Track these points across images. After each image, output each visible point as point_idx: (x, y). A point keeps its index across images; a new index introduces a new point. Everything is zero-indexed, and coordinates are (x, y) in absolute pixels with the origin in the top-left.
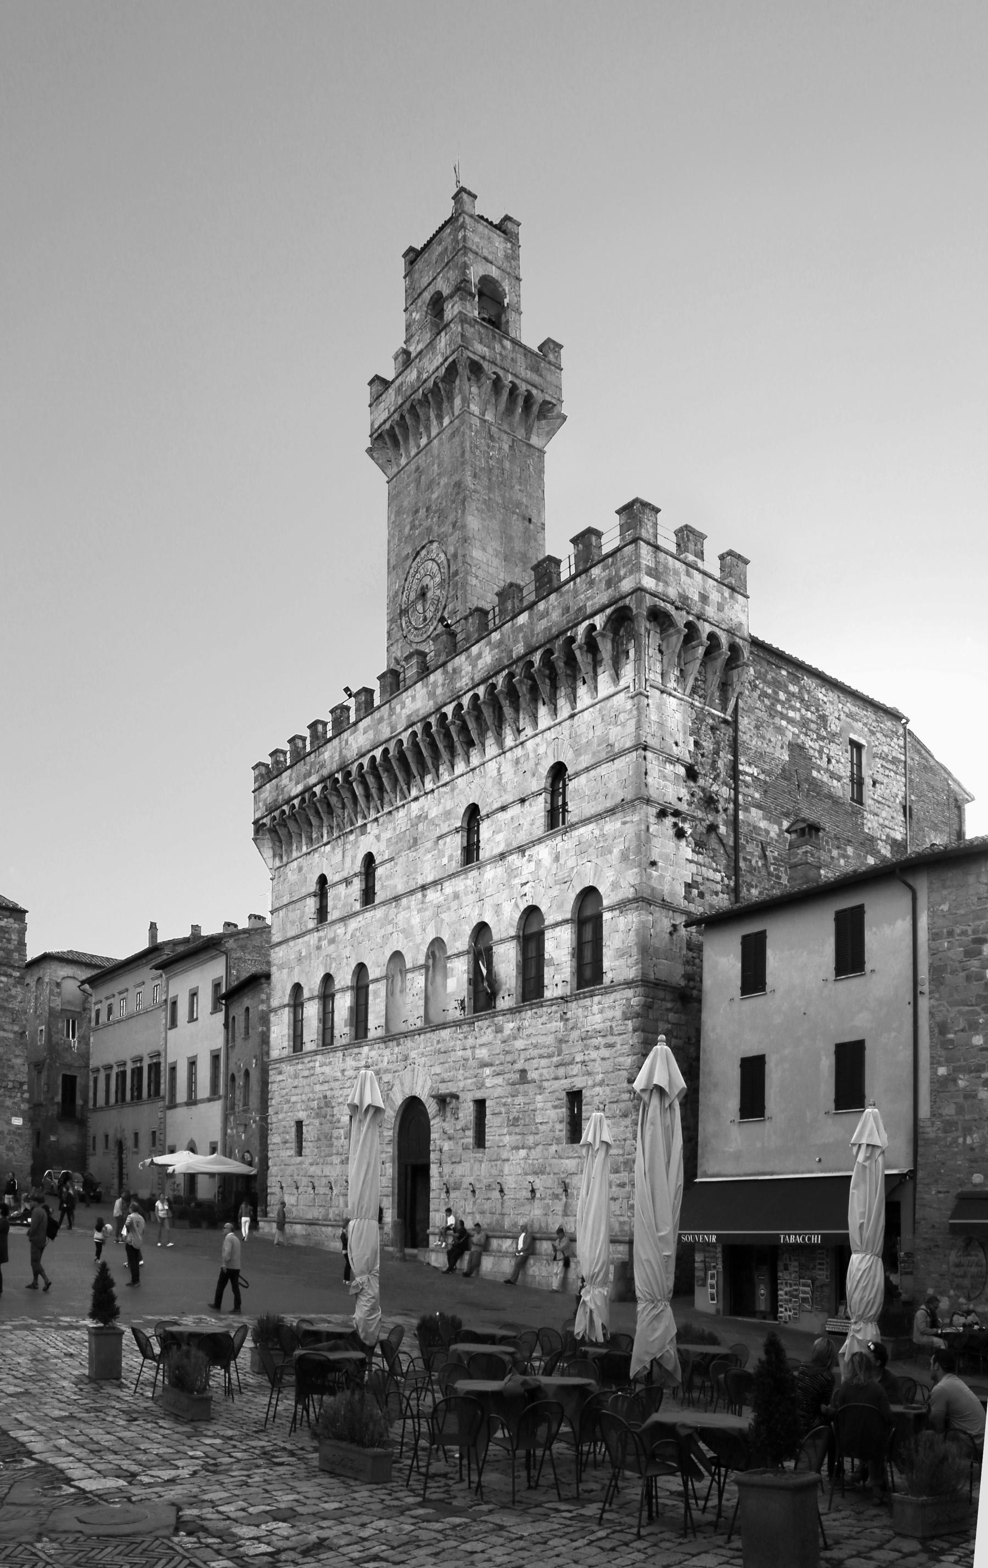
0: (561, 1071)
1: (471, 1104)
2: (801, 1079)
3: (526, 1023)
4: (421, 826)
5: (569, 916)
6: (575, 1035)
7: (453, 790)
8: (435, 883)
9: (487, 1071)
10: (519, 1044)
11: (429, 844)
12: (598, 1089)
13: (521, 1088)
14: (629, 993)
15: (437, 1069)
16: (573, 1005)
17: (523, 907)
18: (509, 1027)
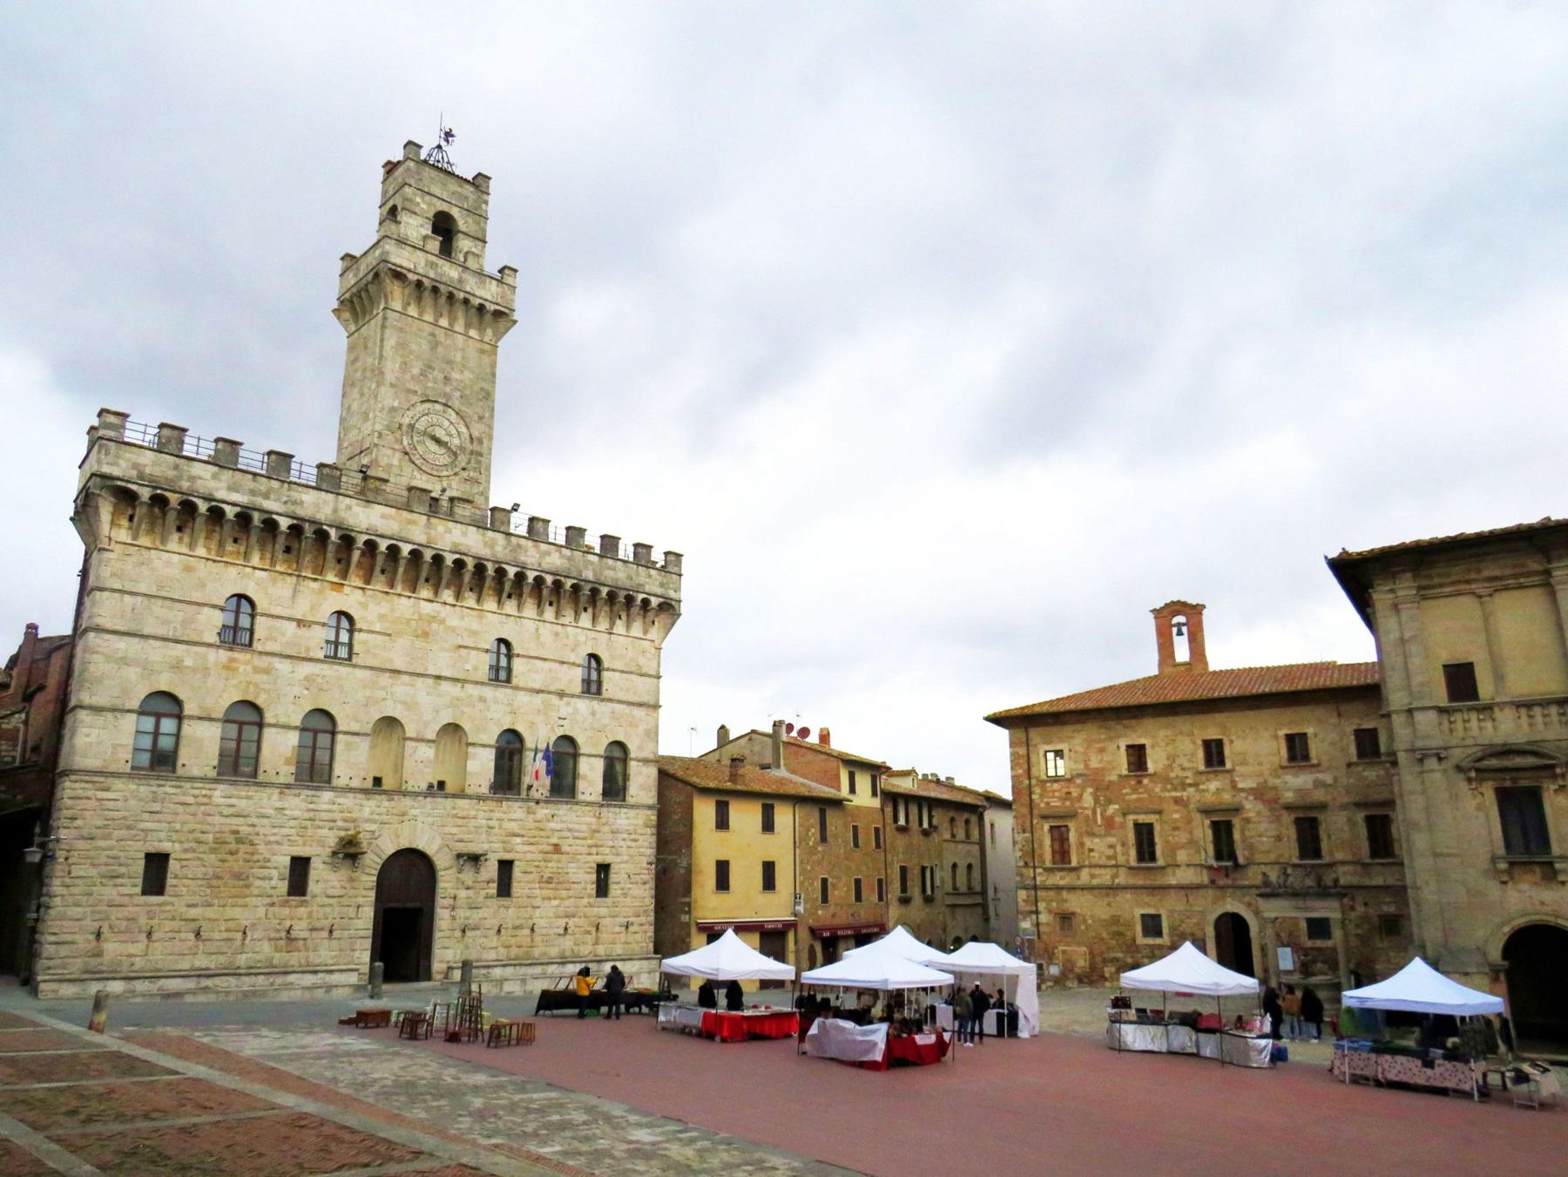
0: (594, 850)
2: (745, 876)
4: (435, 626)
6: (606, 828)
7: (481, 618)
8: (457, 680)
9: (518, 840)
10: (553, 825)
15: (454, 830)
16: (605, 810)
17: (560, 732)
18: (543, 811)
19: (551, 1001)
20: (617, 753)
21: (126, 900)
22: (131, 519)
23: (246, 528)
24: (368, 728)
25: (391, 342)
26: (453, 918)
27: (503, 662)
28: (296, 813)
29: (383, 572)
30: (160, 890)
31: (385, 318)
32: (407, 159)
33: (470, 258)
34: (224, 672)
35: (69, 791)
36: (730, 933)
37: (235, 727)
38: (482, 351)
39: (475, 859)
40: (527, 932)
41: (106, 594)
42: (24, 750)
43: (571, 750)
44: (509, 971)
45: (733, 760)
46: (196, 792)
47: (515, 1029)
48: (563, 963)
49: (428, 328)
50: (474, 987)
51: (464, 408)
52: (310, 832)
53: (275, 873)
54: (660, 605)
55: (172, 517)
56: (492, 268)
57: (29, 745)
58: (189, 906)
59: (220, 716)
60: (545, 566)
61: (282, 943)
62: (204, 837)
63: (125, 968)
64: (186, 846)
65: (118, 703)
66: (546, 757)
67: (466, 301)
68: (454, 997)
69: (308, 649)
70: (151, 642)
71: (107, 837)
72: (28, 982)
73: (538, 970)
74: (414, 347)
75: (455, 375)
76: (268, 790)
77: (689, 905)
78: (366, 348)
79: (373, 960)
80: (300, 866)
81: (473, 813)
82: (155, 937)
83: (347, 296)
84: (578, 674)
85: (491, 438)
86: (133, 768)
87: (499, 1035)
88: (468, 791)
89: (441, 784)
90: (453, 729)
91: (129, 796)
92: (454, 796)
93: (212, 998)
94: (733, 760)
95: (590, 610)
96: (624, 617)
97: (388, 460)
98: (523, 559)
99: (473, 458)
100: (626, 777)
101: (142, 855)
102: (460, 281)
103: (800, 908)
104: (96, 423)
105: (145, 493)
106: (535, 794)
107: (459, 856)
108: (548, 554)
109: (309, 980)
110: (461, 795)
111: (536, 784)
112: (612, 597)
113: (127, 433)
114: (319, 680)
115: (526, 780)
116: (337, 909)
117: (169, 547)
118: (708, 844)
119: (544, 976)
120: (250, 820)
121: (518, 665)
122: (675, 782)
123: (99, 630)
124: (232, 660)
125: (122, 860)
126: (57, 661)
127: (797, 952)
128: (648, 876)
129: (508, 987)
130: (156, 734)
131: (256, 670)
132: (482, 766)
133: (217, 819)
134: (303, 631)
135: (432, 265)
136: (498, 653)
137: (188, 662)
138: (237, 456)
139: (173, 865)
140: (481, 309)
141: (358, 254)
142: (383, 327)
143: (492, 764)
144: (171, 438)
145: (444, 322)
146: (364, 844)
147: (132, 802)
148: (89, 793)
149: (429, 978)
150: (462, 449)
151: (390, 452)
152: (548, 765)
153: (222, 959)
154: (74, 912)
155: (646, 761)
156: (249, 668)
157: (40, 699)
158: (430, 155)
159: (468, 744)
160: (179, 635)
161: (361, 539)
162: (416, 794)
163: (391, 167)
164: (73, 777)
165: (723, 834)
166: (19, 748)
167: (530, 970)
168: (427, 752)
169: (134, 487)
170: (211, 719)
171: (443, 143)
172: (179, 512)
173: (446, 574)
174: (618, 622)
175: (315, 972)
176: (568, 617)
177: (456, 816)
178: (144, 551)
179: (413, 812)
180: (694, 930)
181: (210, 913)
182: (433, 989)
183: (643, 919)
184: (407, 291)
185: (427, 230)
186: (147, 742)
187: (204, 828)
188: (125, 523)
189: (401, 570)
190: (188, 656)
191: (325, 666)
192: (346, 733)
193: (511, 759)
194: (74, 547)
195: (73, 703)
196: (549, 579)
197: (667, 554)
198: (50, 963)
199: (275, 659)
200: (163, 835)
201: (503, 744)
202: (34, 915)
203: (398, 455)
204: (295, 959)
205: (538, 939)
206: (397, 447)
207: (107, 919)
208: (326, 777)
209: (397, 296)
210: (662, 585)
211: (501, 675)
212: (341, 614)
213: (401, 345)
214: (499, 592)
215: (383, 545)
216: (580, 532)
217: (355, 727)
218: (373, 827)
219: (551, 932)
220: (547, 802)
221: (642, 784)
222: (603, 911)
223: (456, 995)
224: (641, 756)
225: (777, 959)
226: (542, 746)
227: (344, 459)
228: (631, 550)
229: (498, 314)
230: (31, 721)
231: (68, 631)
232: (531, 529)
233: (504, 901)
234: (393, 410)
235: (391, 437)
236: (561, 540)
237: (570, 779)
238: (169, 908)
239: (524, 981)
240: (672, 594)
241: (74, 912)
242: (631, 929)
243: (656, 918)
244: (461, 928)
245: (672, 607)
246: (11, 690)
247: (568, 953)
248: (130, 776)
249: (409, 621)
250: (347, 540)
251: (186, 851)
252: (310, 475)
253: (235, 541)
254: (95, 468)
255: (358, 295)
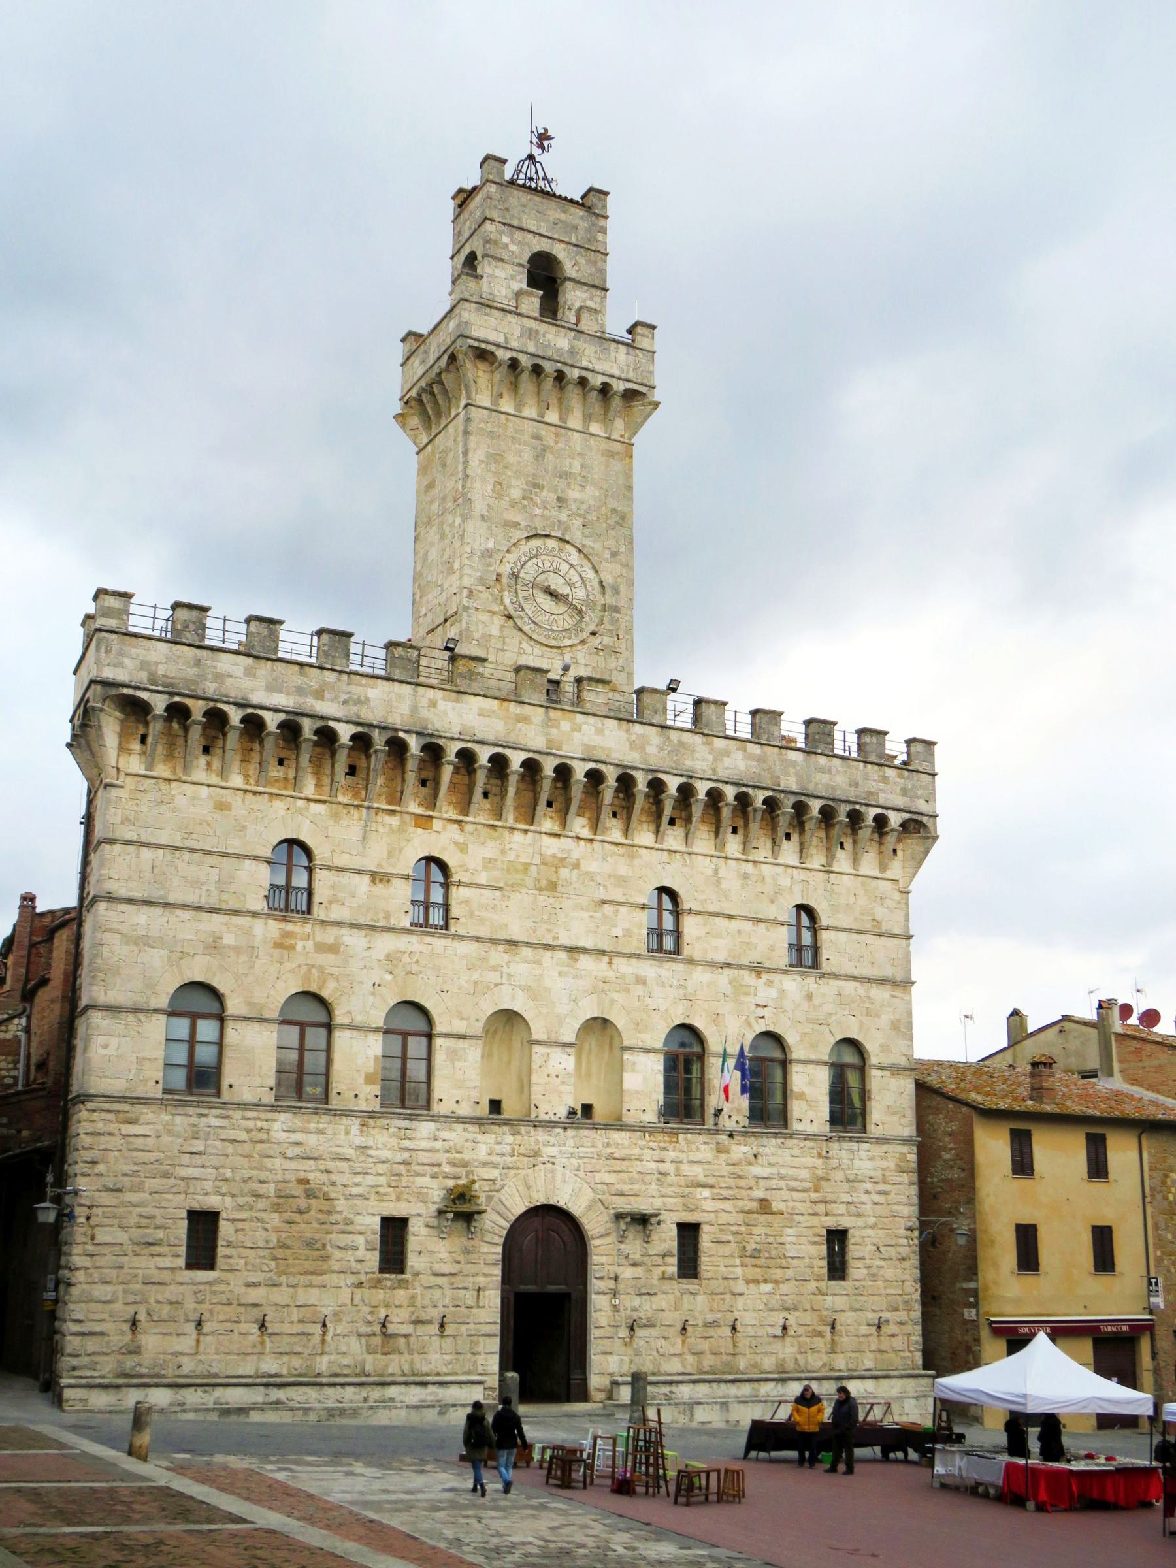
0: (821, 1208)
1: (674, 1227)
3: (767, 1150)
4: (564, 873)
5: (826, 1058)
6: (839, 1175)
7: (632, 857)
8: (599, 952)
9: (706, 1193)
10: (757, 1170)
11: (584, 902)
12: (869, 1232)
13: (763, 1218)
14: (905, 1149)
16: (836, 1145)
17: (760, 1027)
18: (740, 1150)
19: (764, 1437)
20: (850, 1058)
21: (166, 1276)
22: (143, 740)
23: (295, 743)
24: (478, 1028)
25: (477, 457)
26: (616, 1308)
27: (668, 922)
28: (385, 1154)
29: (486, 795)
30: (211, 1265)
31: (468, 420)
32: (486, 181)
33: (585, 316)
34: (276, 952)
35: (86, 1124)
36: (1042, 1339)
37: (295, 1030)
38: (611, 454)
39: (642, 1221)
40: (728, 1331)
41: (117, 848)
42: (28, 1065)
43: (778, 1054)
44: (702, 1390)
45: (1035, 1065)
46: (251, 1124)
47: (713, 1476)
48: (784, 1380)
49: (530, 427)
50: (651, 1413)
51: (587, 542)
52: (404, 1179)
53: (360, 1240)
54: (904, 825)
55: (196, 733)
56: (617, 326)
57: (34, 1060)
58: (249, 1285)
59: (275, 1015)
60: (722, 774)
61: (378, 1340)
62: (262, 1189)
63: (170, 1371)
64: (241, 1200)
65: (140, 1000)
66: (740, 1066)
67: (583, 382)
68: (621, 1426)
69: (387, 916)
70: (179, 912)
71: (139, 1188)
72: (50, 1388)
73: (746, 1390)
74: (510, 458)
75: (574, 494)
76: (345, 1120)
77: (975, 1293)
78: (444, 465)
79: (503, 1368)
80: (394, 1230)
81: (636, 1151)
82: (207, 1327)
83: (414, 393)
84: (783, 937)
85: (630, 583)
86: (165, 1091)
87: (691, 1487)
88: (628, 1119)
89: (587, 1109)
90: (600, 1025)
91: (165, 1128)
92: (607, 1127)
93: (285, 1417)
94: (1035, 1065)
95: (795, 837)
96: (848, 845)
97: (482, 630)
98: (688, 763)
99: (605, 615)
100: (864, 1095)
101: (185, 1215)
102: (572, 352)
103: (1158, 1301)
104: (91, 608)
105: (159, 704)
106: (727, 1123)
107: (619, 1217)
108: (727, 753)
109: (415, 1395)
110: (616, 1124)
111: (727, 1107)
112: (827, 814)
113: (133, 620)
114: (406, 959)
115: (714, 1100)
116: (449, 1293)
117: (194, 778)
118: (1001, 1202)
119: (755, 1400)
120: (323, 1165)
121: (690, 926)
122: (941, 1099)
123: (110, 898)
124: (287, 935)
125: (159, 1221)
126: (62, 940)
127: (1156, 1371)
128: (908, 1248)
129: (701, 1414)
130: (192, 1042)
131: (321, 948)
132: (644, 1082)
133: (278, 1163)
134: (379, 889)
135: (531, 334)
136: (660, 909)
137: (229, 939)
138: (276, 640)
139: (225, 1229)
140: (605, 390)
141: (425, 332)
142: (466, 433)
143: (660, 1079)
144: (188, 622)
145: (552, 417)
146: (482, 1200)
147: (166, 1139)
148: (113, 1127)
149: (584, 1397)
150: (591, 603)
151: (485, 617)
152: (743, 1077)
153: (296, 1362)
154: (100, 1291)
155: (895, 1070)
156: (310, 945)
157: (43, 995)
158: (518, 172)
159: (624, 1049)
160: (213, 902)
161: (452, 749)
162: (553, 1124)
163: (464, 198)
164: (90, 1105)
165: (1023, 1183)
166: (21, 1065)
167: (733, 1390)
168: (563, 1062)
169: (144, 695)
170: (263, 1020)
171: (536, 151)
172: (205, 727)
173: (577, 792)
174: (840, 853)
175: (424, 1384)
176: (763, 850)
177: (611, 1157)
178: (163, 785)
179: (549, 1151)
180: (985, 1333)
181: (280, 1296)
182: (590, 1415)
183: (902, 1315)
184: (497, 376)
185: (521, 283)
186: (180, 1054)
187: (263, 1175)
188: (136, 746)
189: (511, 791)
190: (228, 930)
191: (414, 939)
192: (448, 1036)
193: (688, 1070)
194: (73, 784)
195: (84, 1001)
196: (730, 792)
197: (909, 742)
198: (75, 1362)
199: (345, 931)
200: (209, 1186)
201: (674, 1047)
202: (51, 1295)
203: (499, 620)
204: (394, 1365)
205: (743, 1343)
206: (496, 608)
207: (144, 1301)
208: (423, 1102)
209: (482, 384)
210: (904, 792)
211: (666, 942)
212: (430, 860)
213: (496, 457)
214: (656, 816)
215: (484, 755)
216: (774, 716)
217: (459, 1027)
218: (494, 1173)
219: (761, 1332)
220: (745, 1134)
221: (890, 1104)
222: (840, 1302)
223: (625, 1424)
224: (887, 1060)
225: (1123, 1381)
226: (734, 1050)
227: (422, 632)
228: (853, 739)
229: (630, 395)
230: (34, 1029)
231: (72, 901)
232: (697, 719)
233: (689, 1285)
234: (487, 554)
235: (486, 595)
236: (745, 731)
237: (778, 1099)
238: (223, 1287)
239: (725, 1405)
240: (922, 806)
241: (100, 1291)
242: (885, 1329)
243: (924, 1314)
244: (629, 1321)
245: (924, 826)
246: (7, 987)
247: (790, 1365)
248: (161, 1102)
249: (526, 866)
250: (433, 752)
251: (241, 1207)
252: (376, 659)
253: (281, 762)
254: (93, 674)
255: (429, 390)
